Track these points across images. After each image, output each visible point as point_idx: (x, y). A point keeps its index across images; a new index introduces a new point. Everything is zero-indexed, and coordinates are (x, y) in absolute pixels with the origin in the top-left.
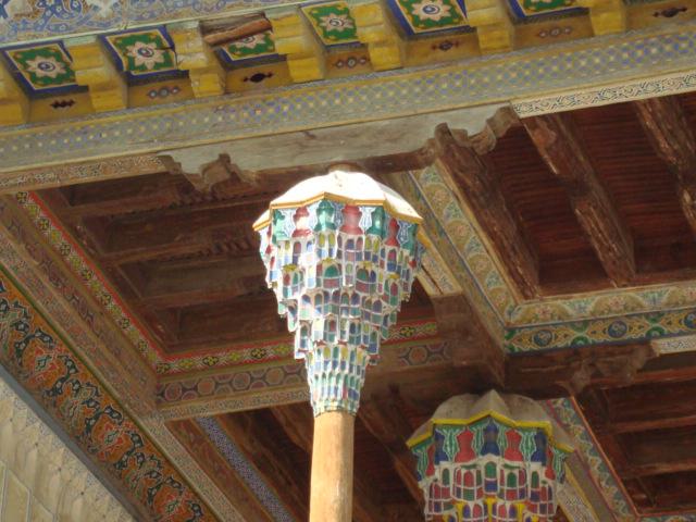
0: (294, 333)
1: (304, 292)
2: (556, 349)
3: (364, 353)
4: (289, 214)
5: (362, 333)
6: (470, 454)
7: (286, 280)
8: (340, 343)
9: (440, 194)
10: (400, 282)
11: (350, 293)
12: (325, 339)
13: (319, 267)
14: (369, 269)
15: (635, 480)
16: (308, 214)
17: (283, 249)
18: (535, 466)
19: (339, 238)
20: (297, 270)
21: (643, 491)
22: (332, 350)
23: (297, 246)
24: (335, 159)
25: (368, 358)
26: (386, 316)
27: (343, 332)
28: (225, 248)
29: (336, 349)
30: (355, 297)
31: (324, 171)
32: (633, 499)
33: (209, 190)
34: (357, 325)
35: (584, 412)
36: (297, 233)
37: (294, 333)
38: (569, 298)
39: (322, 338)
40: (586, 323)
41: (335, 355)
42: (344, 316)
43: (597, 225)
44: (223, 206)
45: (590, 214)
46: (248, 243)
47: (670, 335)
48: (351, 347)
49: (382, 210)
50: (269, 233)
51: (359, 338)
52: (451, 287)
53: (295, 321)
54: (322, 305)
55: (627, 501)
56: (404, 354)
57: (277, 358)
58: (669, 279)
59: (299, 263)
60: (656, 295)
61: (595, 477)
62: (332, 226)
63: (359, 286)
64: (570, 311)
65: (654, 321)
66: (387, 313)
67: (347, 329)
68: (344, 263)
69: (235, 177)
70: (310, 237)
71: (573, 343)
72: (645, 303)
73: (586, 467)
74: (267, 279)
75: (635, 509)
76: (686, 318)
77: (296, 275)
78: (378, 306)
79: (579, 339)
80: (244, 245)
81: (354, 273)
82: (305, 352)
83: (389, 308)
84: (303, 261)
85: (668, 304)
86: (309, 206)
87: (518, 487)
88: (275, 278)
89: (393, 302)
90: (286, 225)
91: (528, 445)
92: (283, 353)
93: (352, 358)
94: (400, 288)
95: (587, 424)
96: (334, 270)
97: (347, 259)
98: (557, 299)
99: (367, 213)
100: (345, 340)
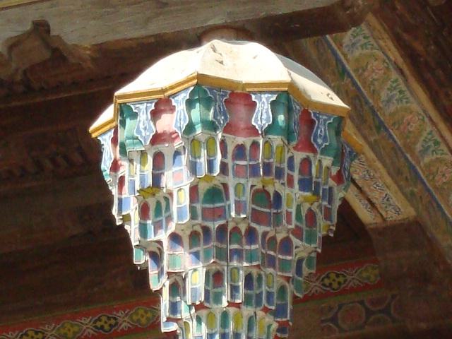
0: (159, 292)
1: (172, 228)
3: (269, 319)
4: (144, 111)
5: (264, 288)
7: (144, 211)
8: (231, 304)
9: (376, 69)
10: (320, 206)
11: (243, 227)
12: (207, 298)
13: (194, 190)
14: (271, 190)
16: (172, 109)
17: (137, 165)
19: (223, 143)
20: (160, 196)
22: (219, 317)
23: (159, 160)
24: (211, 23)
25: (275, 326)
26: (300, 262)
27: (234, 289)
28: (48, 164)
29: (225, 315)
30: (251, 233)
31: (193, 40)
33: (19, 78)
34: (255, 276)
36: (157, 139)
37: (159, 292)
39: (202, 298)
41: (224, 324)
42: (235, 263)
44: (39, 99)
46: (83, 154)
48: (247, 311)
49: (287, 97)
50: (114, 141)
51: (259, 296)
52: (398, 212)
53: (160, 273)
54: (201, 248)
56: (330, 315)
57: (135, 330)
59: (163, 184)
62: (211, 126)
63: (256, 217)
66: (304, 255)
67: (241, 284)
68: (231, 181)
69: (59, 55)
70: (178, 144)
74: (115, 211)
77: (158, 203)
78: (286, 246)
80: (77, 158)
81: (247, 197)
82: (177, 320)
83: (303, 249)
84: (168, 181)
86: (174, 95)
88: (127, 209)
89: (310, 239)
90: (141, 126)
92: (144, 321)
93: (250, 328)
94: (320, 217)
96: (217, 194)
97: (236, 174)
99: (263, 105)
100: (238, 301)
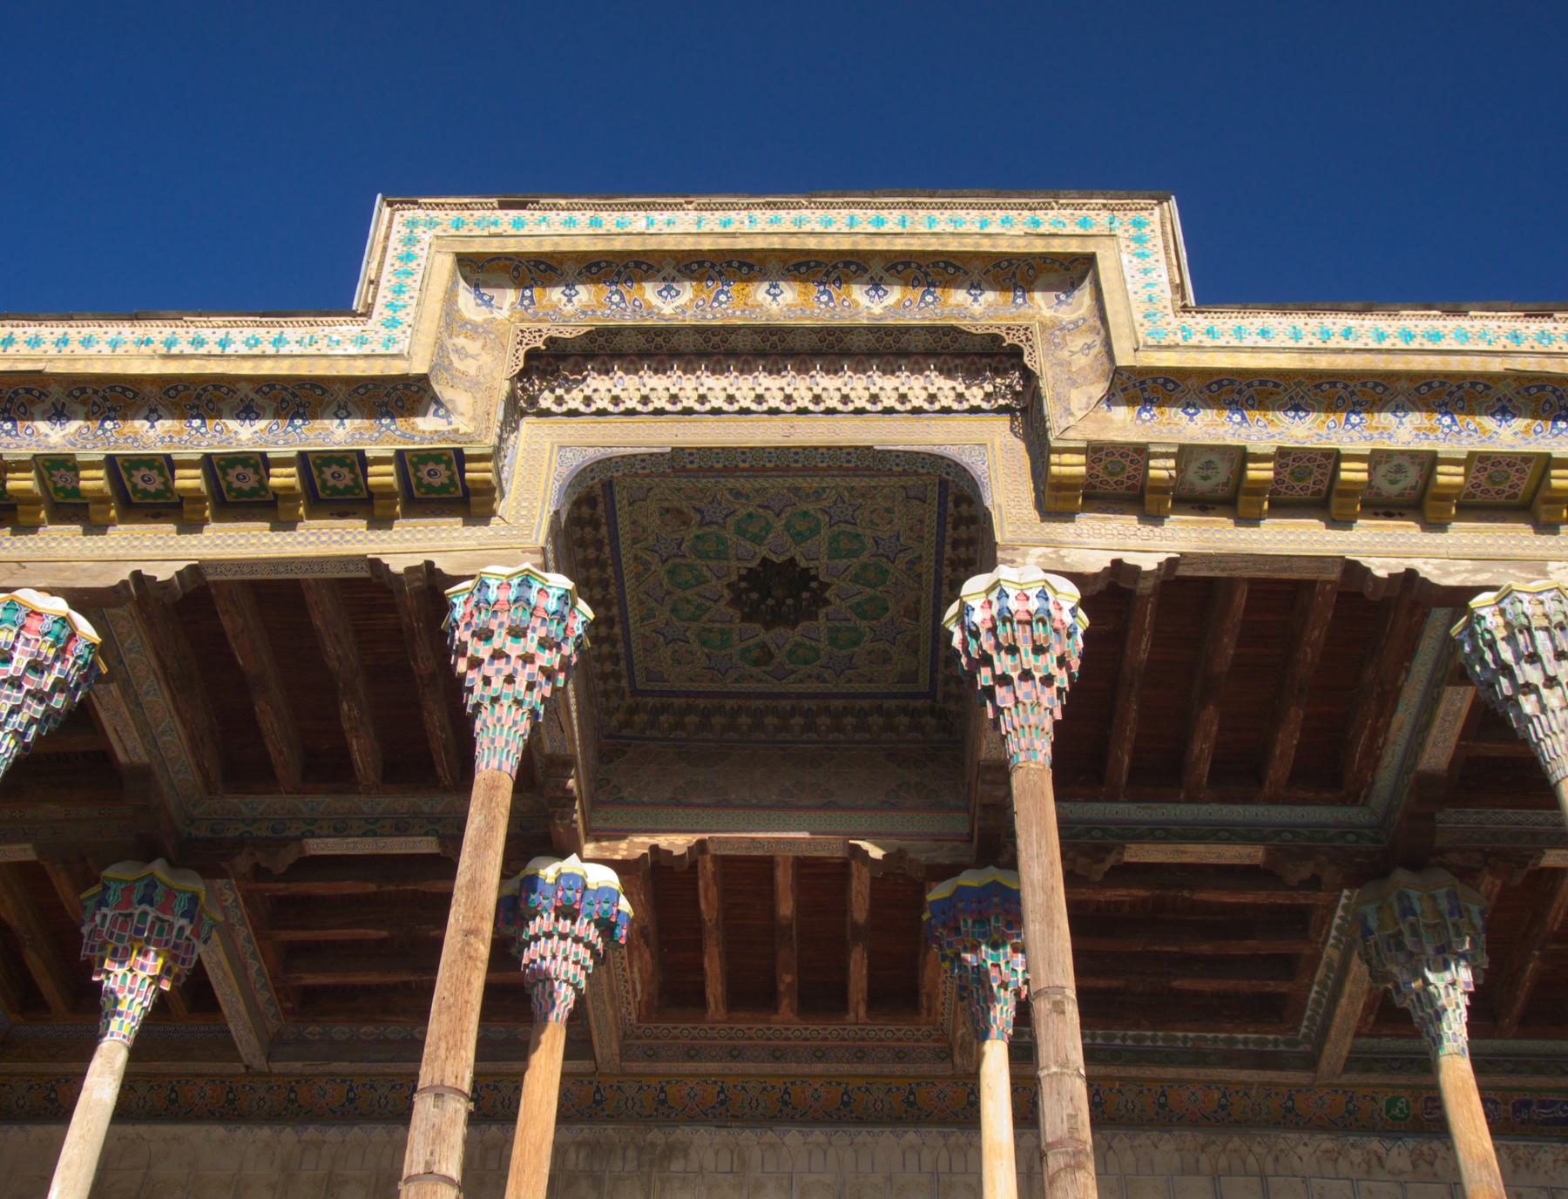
6: (129, 904)
18: (183, 922)
40: (255, 821)
73: (245, 967)
87: (165, 937)
91: (181, 904)
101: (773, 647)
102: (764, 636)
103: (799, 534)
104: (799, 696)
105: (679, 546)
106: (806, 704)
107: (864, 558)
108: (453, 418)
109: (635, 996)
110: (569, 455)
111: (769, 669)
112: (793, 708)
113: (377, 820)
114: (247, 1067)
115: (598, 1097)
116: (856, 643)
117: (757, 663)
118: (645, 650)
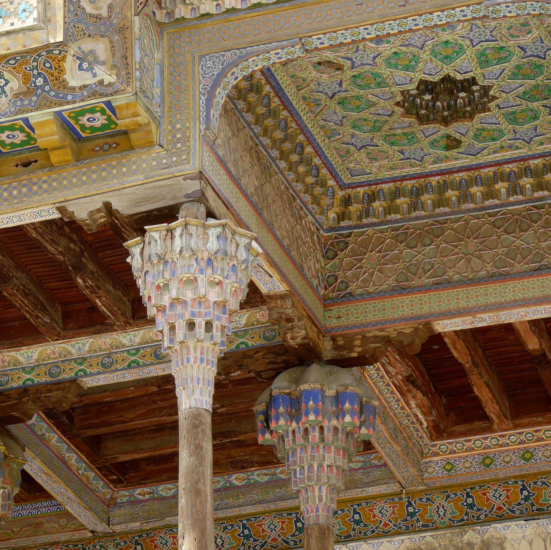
2: (13, 389)
15: (105, 466)
21: (114, 474)
32: (108, 479)
35: (54, 424)
38: (19, 350)
40: (33, 368)
43: (22, 302)
45: (15, 295)
47: (92, 375)
55: (103, 480)
58: (88, 334)
60: (81, 345)
61: (74, 470)
64: (22, 359)
65: (80, 364)
71: (24, 383)
72: (73, 351)
75: (111, 486)
76: (102, 361)
79: (28, 380)
85: (89, 352)
95: (58, 432)
98: (10, 351)
101: (457, 136)
102: (444, 130)
103: (446, 58)
104: (498, 164)
105: (340, 84)
106: (507, 168)
107: (515, 61)
108: (97, 69)
109: (421, 424)
110: (210, 64)
111: (460, 150)
112: (495, 173)
113: (138, 350)
114: (92, 532)
115: (411, 510)
116: (536, 118)
117: (448, 148)
118: (341, 156)
